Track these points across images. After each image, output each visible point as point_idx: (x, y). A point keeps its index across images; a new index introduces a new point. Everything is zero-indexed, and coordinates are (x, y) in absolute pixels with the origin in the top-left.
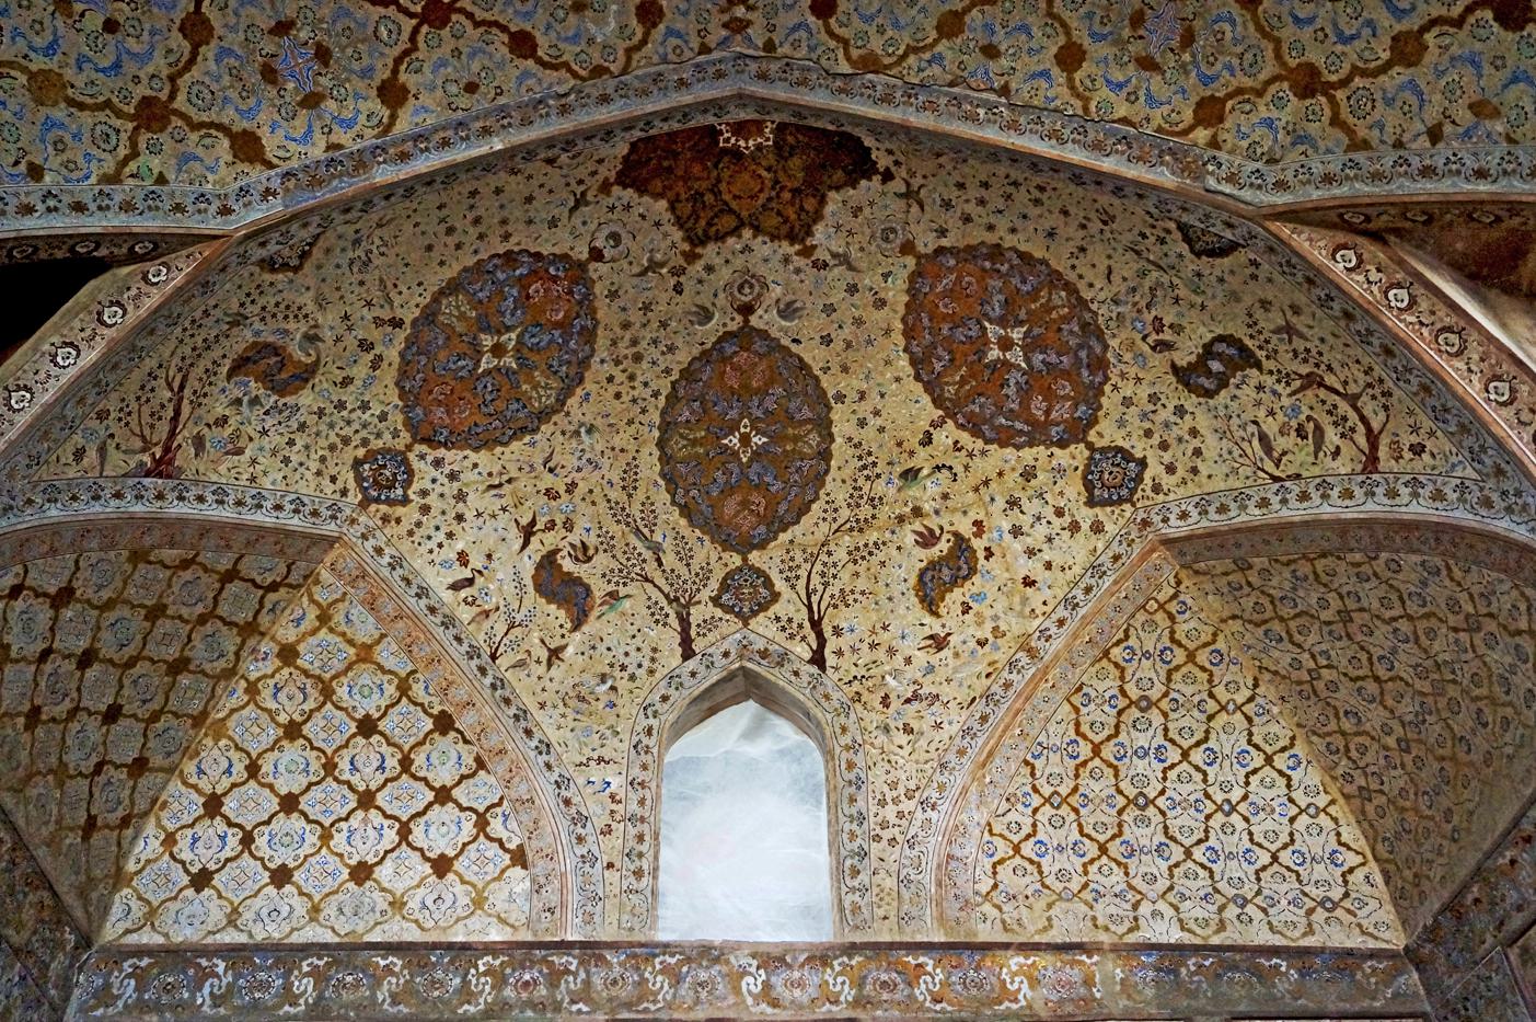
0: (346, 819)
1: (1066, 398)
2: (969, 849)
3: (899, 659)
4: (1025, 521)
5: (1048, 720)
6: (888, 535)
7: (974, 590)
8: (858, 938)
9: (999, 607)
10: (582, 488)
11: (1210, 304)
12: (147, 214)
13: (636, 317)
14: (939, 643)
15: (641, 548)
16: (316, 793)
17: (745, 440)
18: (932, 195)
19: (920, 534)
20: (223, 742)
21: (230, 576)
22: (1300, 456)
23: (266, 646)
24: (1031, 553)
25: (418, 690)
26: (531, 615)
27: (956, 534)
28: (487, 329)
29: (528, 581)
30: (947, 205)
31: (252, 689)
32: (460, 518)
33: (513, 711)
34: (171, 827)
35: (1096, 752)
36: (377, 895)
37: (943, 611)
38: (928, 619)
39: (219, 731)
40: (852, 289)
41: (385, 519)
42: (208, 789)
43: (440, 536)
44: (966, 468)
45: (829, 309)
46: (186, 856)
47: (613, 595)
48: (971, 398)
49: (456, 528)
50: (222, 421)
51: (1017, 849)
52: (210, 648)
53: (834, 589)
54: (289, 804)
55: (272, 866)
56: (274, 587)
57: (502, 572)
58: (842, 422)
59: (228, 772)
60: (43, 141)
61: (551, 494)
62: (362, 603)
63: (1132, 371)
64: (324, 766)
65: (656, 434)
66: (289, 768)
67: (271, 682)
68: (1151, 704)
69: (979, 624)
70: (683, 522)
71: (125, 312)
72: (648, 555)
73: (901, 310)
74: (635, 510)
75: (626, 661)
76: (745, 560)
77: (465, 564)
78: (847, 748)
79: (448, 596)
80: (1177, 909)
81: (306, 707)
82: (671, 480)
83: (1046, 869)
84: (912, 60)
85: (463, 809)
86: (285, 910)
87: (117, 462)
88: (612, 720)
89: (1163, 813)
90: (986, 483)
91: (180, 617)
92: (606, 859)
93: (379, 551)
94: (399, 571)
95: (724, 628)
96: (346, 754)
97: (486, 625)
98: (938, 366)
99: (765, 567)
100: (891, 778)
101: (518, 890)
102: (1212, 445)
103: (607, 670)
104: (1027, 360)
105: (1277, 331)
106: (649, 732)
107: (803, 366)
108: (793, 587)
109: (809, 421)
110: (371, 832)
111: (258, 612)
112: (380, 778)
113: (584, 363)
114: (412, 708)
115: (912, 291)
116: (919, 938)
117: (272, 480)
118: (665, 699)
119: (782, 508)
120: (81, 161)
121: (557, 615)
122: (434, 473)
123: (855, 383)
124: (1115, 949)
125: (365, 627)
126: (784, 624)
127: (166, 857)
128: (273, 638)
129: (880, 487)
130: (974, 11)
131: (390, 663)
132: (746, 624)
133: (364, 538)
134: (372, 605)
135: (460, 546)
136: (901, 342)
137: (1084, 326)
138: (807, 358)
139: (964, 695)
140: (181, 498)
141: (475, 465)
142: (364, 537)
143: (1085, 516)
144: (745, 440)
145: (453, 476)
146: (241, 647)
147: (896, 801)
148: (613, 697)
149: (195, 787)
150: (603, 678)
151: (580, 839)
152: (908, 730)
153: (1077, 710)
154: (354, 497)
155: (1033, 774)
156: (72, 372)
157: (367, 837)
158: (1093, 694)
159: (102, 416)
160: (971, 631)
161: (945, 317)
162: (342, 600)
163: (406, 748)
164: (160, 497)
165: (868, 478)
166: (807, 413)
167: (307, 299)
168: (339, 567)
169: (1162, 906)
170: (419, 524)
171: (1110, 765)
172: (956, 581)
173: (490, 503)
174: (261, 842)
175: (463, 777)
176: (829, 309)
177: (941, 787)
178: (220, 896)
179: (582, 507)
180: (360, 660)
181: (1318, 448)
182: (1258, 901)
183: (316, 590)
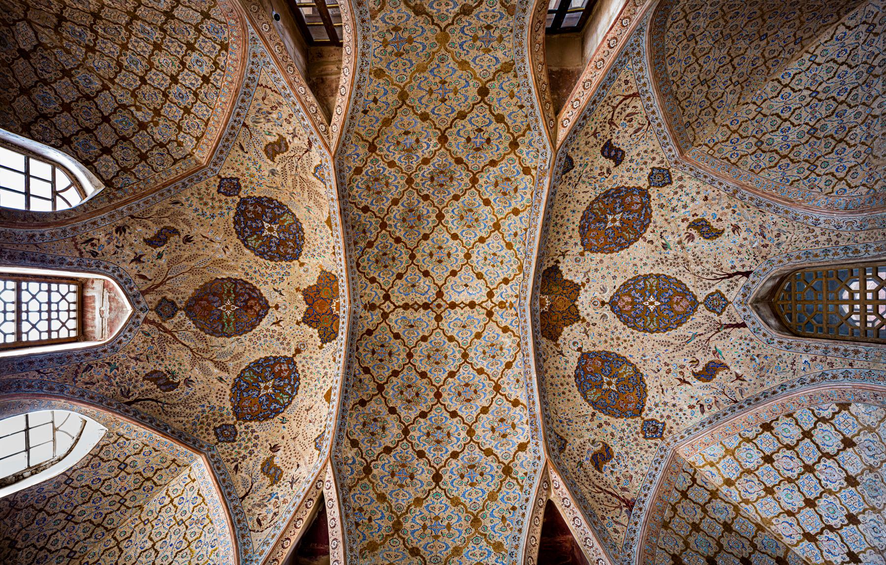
1: (632, 199)
4: (680, 204)
11: (591, 160)
13: (603, 338)
17: (653, 303)
18: (562, 247)
20: (773, 521)
22: (639, 118)
24: (693, 200)
26: (720, 385)
28: (601, 386)
29: (705, 384)
30: (566, 243)
31: (747, 502)
32: (674, 405)
33: (762, 398)
43: (681, 413)
45: (603, 277)
47: (714, 353)
49: (678, 408)
57: (700, 393)
61: (668, 372)
63: (619, 179)
67: (742, 493)
70: (684, 325)
72: (697, 339)
73: (603, 255)
74: (678, 342)
81: (757, 482)
84: (519, 256)
88: (774, 358)
95: (733, 311)
97: (721, 402)
98: (623, 241)
102: (642, 148)
103: (749, 358)
104: (619, 213)
105: (596, 137)
107: (624, 285)
113: (618, 356)
114: (758, 439)
115: (597, 252)
119: (679, 290)
121: (721, 375)
135: (686, 407)
136: (615, 253)
137: (605, 197)
143: (676, 184)
151: (834, 377)
167: (578, 441)
175: (797, 424)
176: (603, 277)
179: (675, 361)
180: (733, 454)
181: (635, 113)
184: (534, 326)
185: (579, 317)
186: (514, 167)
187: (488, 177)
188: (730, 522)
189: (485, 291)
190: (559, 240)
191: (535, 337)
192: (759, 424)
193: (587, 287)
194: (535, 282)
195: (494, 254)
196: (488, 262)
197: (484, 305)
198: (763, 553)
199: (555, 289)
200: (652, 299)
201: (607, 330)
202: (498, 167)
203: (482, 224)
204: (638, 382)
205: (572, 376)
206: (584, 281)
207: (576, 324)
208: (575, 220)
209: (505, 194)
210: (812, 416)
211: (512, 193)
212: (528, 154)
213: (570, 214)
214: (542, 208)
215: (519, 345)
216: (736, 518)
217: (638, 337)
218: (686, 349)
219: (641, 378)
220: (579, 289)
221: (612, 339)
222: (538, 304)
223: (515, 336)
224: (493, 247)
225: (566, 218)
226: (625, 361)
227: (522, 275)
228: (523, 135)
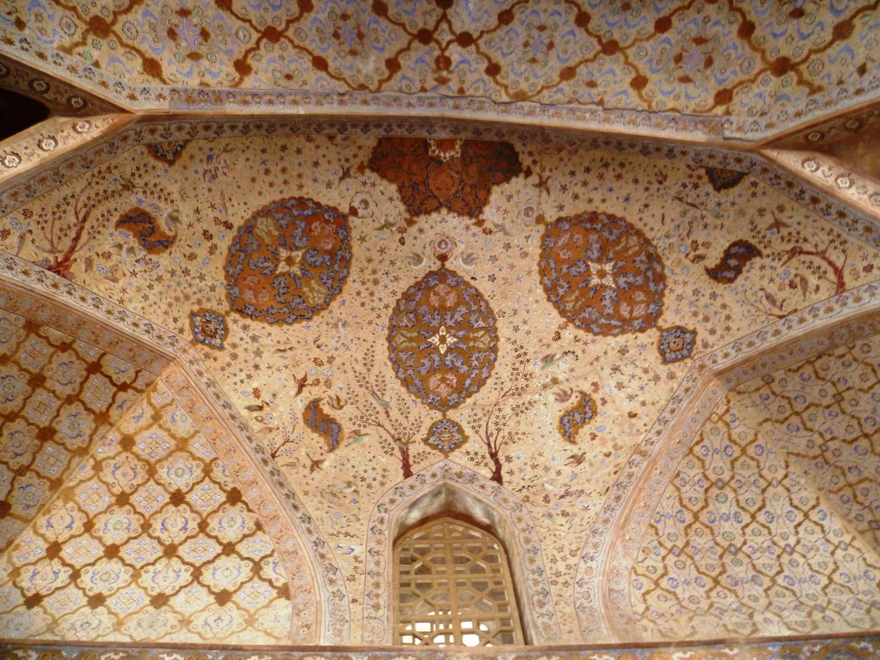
0: (153, 564)
2: (623, 585)
3: (552, 474)
5: (661, 496)
6: (537, 397)
7: (597, 424)
8: (552, 644)
9: (615, 433)
10: (338, 361)
12: (84, 78)
14: (578, 460)
15: (374, 402)
16: (133, 545)
17: (443, 341)
19: (559, 395)
20: (70, 505)
21: (94, 368)
23: (114, 436)
25: (217, 473)
27: (581, 393)
30: (564, 188)
31: (98, 467)
32: (256, 367)
33: (285, 491)
34: (18, 564)
35: (695, 518)
36: (170, 615)
37: (578, 440)
38: (569, 446)
39: (68, 496)
40: (508, 246)
41: (207, 356)
42: (52, 538)
43: (243, 376)
44: (584, 351)
45: (494, 259)
46: (25, 584)
47: (355, 432)
48: (582, 309)
49: (253, 372)
50: (108, 256)
51: (657, 583)
52: (71, 427)
53: (505, 432)
54: (112, 552)
55: (91, 594)
56: (124, 387)
58: (504, 329)
59: (70, 526)
60: (30, 10)
62: (184, 407)
64: (142, 526)
65: (386, 332)
66: (116, 526)
67: (112, 462)
68: (727, 484)
69: (604, 442)
70: (403, 390)
71: (57, 143)
72: (380, 409)
73: (537, 258)
74: (372, 379)
75: (365, 476)
76: (444, 416)
77: (258, 397)
78: (524, 530)
79: (245, 413)
80: (780, 616)
81: (135, 482)
82: (396, 363)
83: (681, 596)
85: (243, 559)
86: (95, 623)
87: (29, 251)
89: (749, 556)
90: (597, 359)
91: (54, 392)
92: (351, 596)
93: (200, 373)
94: (212, 389)
96: (159, 518)
97: (270, 436)
98: (561, 292)
99: (457, 420)
100: (557, 545)
101: (282, 613)
103: (352, 479)
106: (382, 521)
107: (478, 296)
108: (477, 432)
109: (482, 328)
110: (171, 574)
111: (110, 406)
112: (183, 536)
114: (212, 485)
115: (544, 247)
116: (599, 642)
117: (134, 306)
118: (392, 501)
119: (468, 382)
120: (50, 31)
121: (316, 441)
122: (243, 335)
123: (510, 304)
124: (749, 642)
125: (183, 427)
126: (473, 457)
127: (10, 584)
128: (118, 429)
129: (530, 368)
130: (582, 67)
131: (198, 454)
132: (446, 456)
133: (188, 362)
134: (191, 410)
135: (255, 385)
136: (537, 277)
138: (481, 289)
139: (601, 488)
140: (69, 293)
141: (270, 334)
142: (191, 362)
144: (443, 340)
145: (254, 339)
146: (94, 433)
147: (564, 559)
148: (355, 496)
149: (43, 536)
150: (349, 484)
152: (565, 514)
153: (679, 490)
154: (188, 336)
155: (657, 534)
156: (13, 172)
157: (167, 576)
158: (687, 479)
159: (27, 214)
160: (599, 449)
161: (564, 261)
162: (170, 404)
163: (204, 515)
164: (55, 286)
165: (522, 362)
166: (481, 323)
168: (171, 380)
169: (768, 615)
170: (229, 365)
171: (707, 527)
172: (584, 422)
173: (277, 361)
174: (85, 579)
175: (245, 536)
176: (494, 259)
177: (596, 546)
178: (45, 612)
179: (338, 373)
182: (831, 606)
183: (152, 394)
184: (401, 121)
185: (417, 214)
186: (734, 72)
187: (717, 23)
188: (56, 438)
189: (473, 29)
190: (573, 173)
191: (379, 121)
192: (239, 487)
193: (475, 229)
194: (490, 125)
195: (551, 46)
196: (535, 33)
197: (444, 26)
198: (12, 484)
199: (473, 169)
200: (451, 340)
201: (392, 263)
202: (738, 41)
203: (616, 18)
204: (292, 309)
205: (303, 193)
206: (488, 225)
207: (402, 207)
208: (608, 204)
209: (678, 59)
210: (262, 554)
211: (680, 73)
212: (761, 95)
213: (624, 193)
214: (644, 131)
215: (362, 87)
216: (66, 449)
217: (379, 316)
218: (361, 391)
219: (302, 317)
220: (471, 215)
221: (374, 272)
222: (443, 135)
223: (381, 82)
224: (568, 42)
225: (616, 185)
226: (335, 289)
227: (506, 99)
228: (801, 82)
